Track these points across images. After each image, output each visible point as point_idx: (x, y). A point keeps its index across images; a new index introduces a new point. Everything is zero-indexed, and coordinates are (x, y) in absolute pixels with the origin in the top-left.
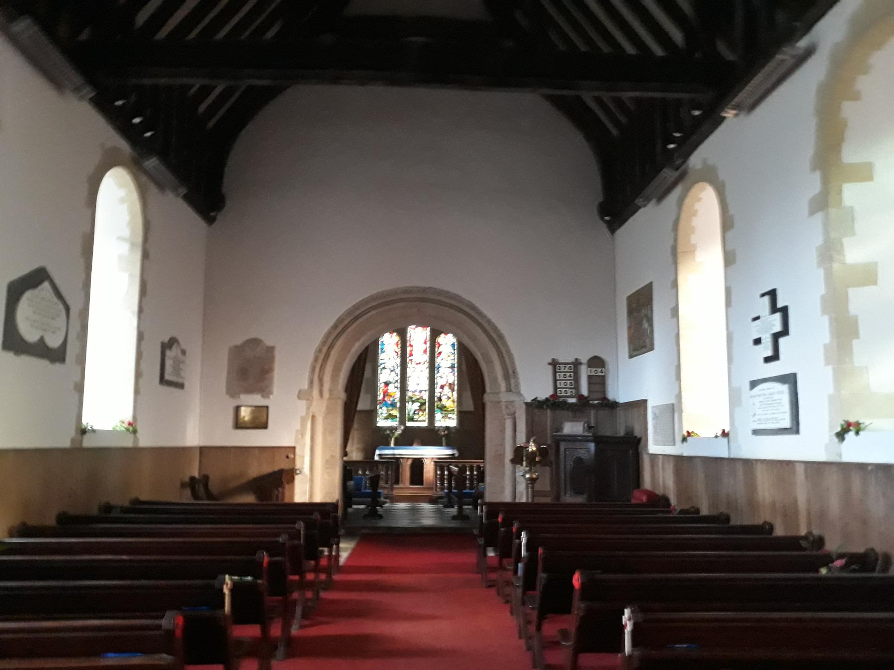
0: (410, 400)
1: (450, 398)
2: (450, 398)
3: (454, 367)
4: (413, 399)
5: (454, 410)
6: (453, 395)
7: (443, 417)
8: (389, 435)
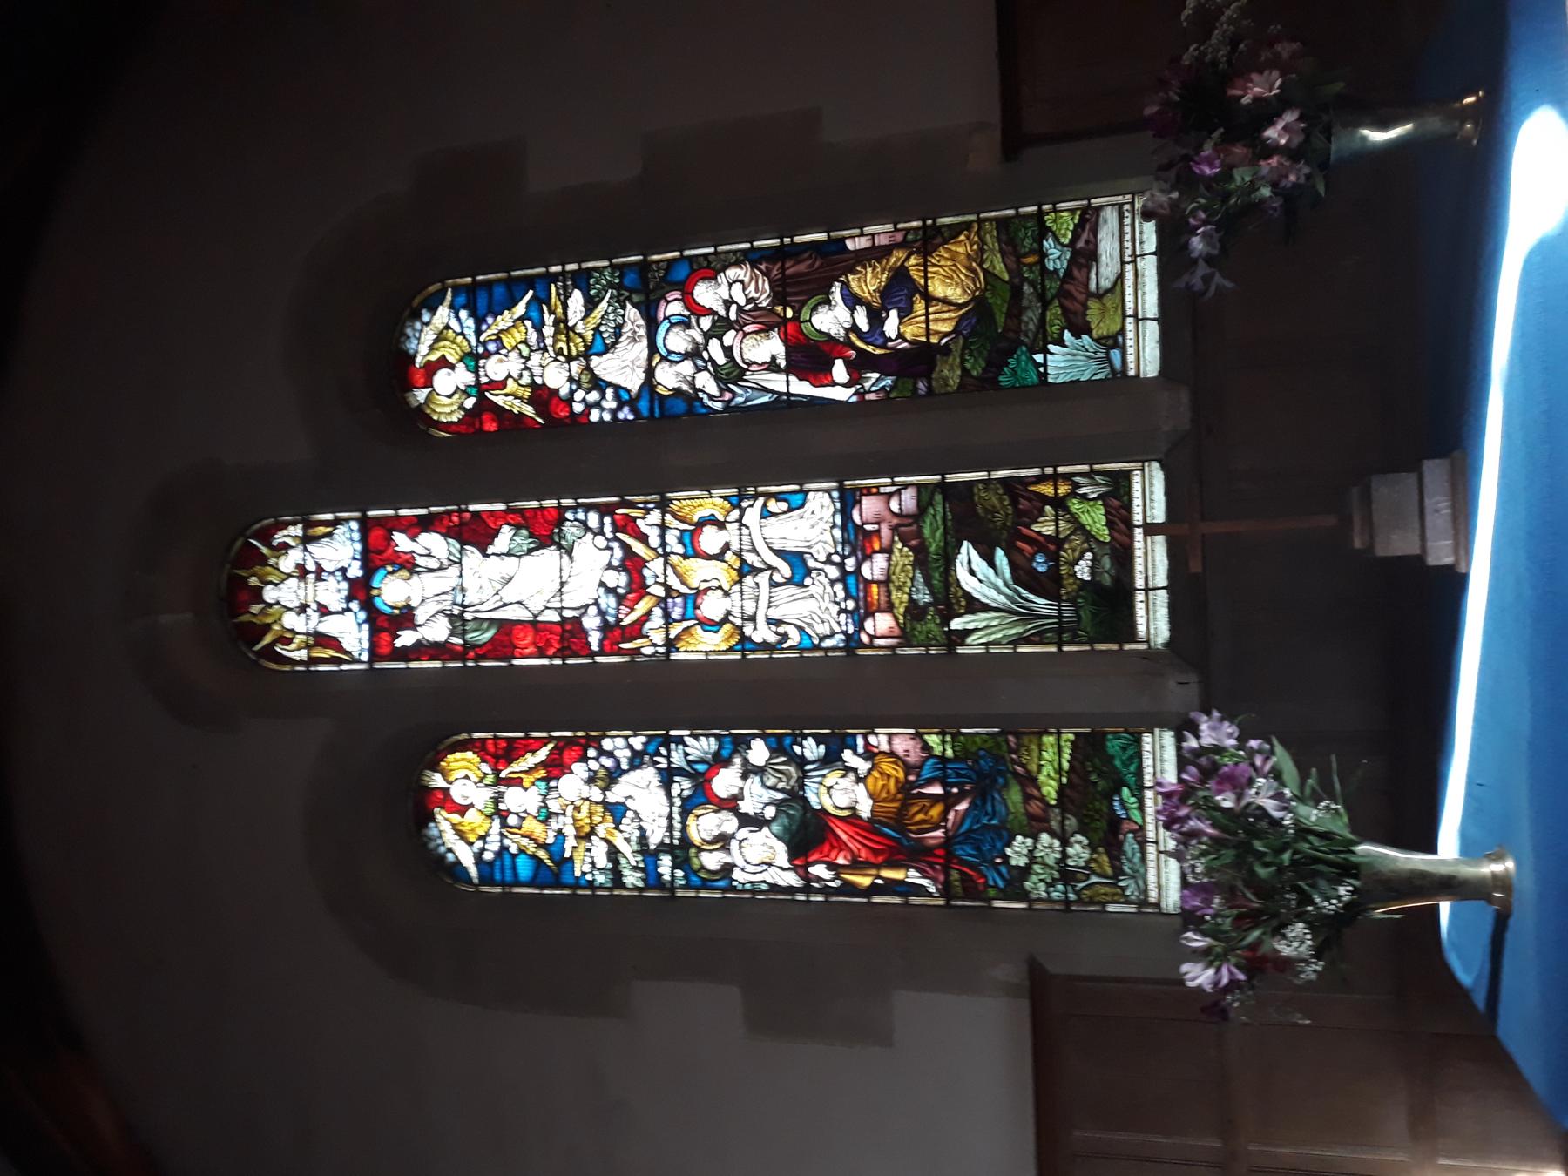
0: (931, 624)
1: (900, 277)
2: (900, 277)
3: (644, 267)
4: (924, 597)
5: (1002, 223)
6: (875, 254)
7: (1080, 328)
8: (1329, 932)
